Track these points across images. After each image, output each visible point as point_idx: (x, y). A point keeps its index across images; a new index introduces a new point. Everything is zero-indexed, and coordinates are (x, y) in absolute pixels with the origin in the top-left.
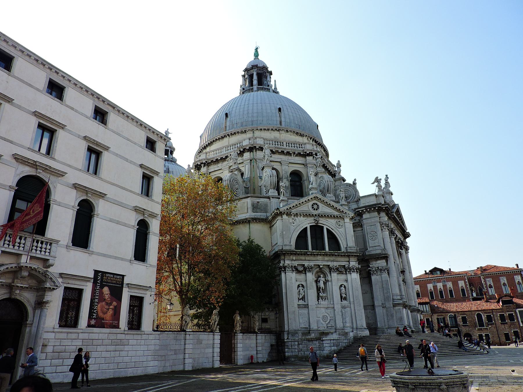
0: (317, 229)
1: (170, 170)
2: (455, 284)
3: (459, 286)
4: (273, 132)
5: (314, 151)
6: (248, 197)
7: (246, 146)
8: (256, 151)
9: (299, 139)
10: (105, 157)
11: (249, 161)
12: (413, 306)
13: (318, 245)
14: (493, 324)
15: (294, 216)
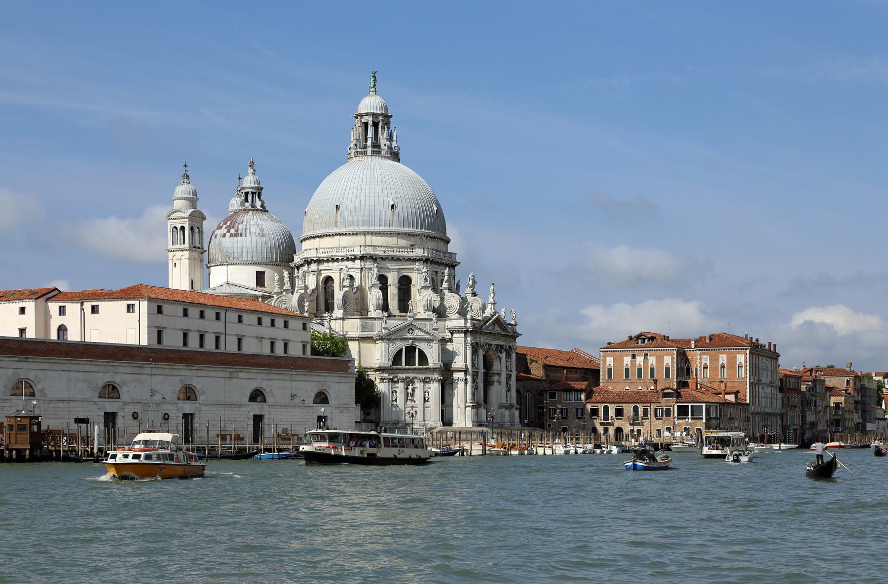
0: (410, 350)
1: (266, 231)
2: (660, 360)
3: (663, 363)
4: (384, 235)
5: (424, 256)
6: (357, 319)
7: (357, 255)
8: (367, 259)
9: (412, 240)
10: (290, 346)
11: (360, 270)
12: (502, 403)
13: (410, 360)
14: (648, 419)
15: (393, 340)
